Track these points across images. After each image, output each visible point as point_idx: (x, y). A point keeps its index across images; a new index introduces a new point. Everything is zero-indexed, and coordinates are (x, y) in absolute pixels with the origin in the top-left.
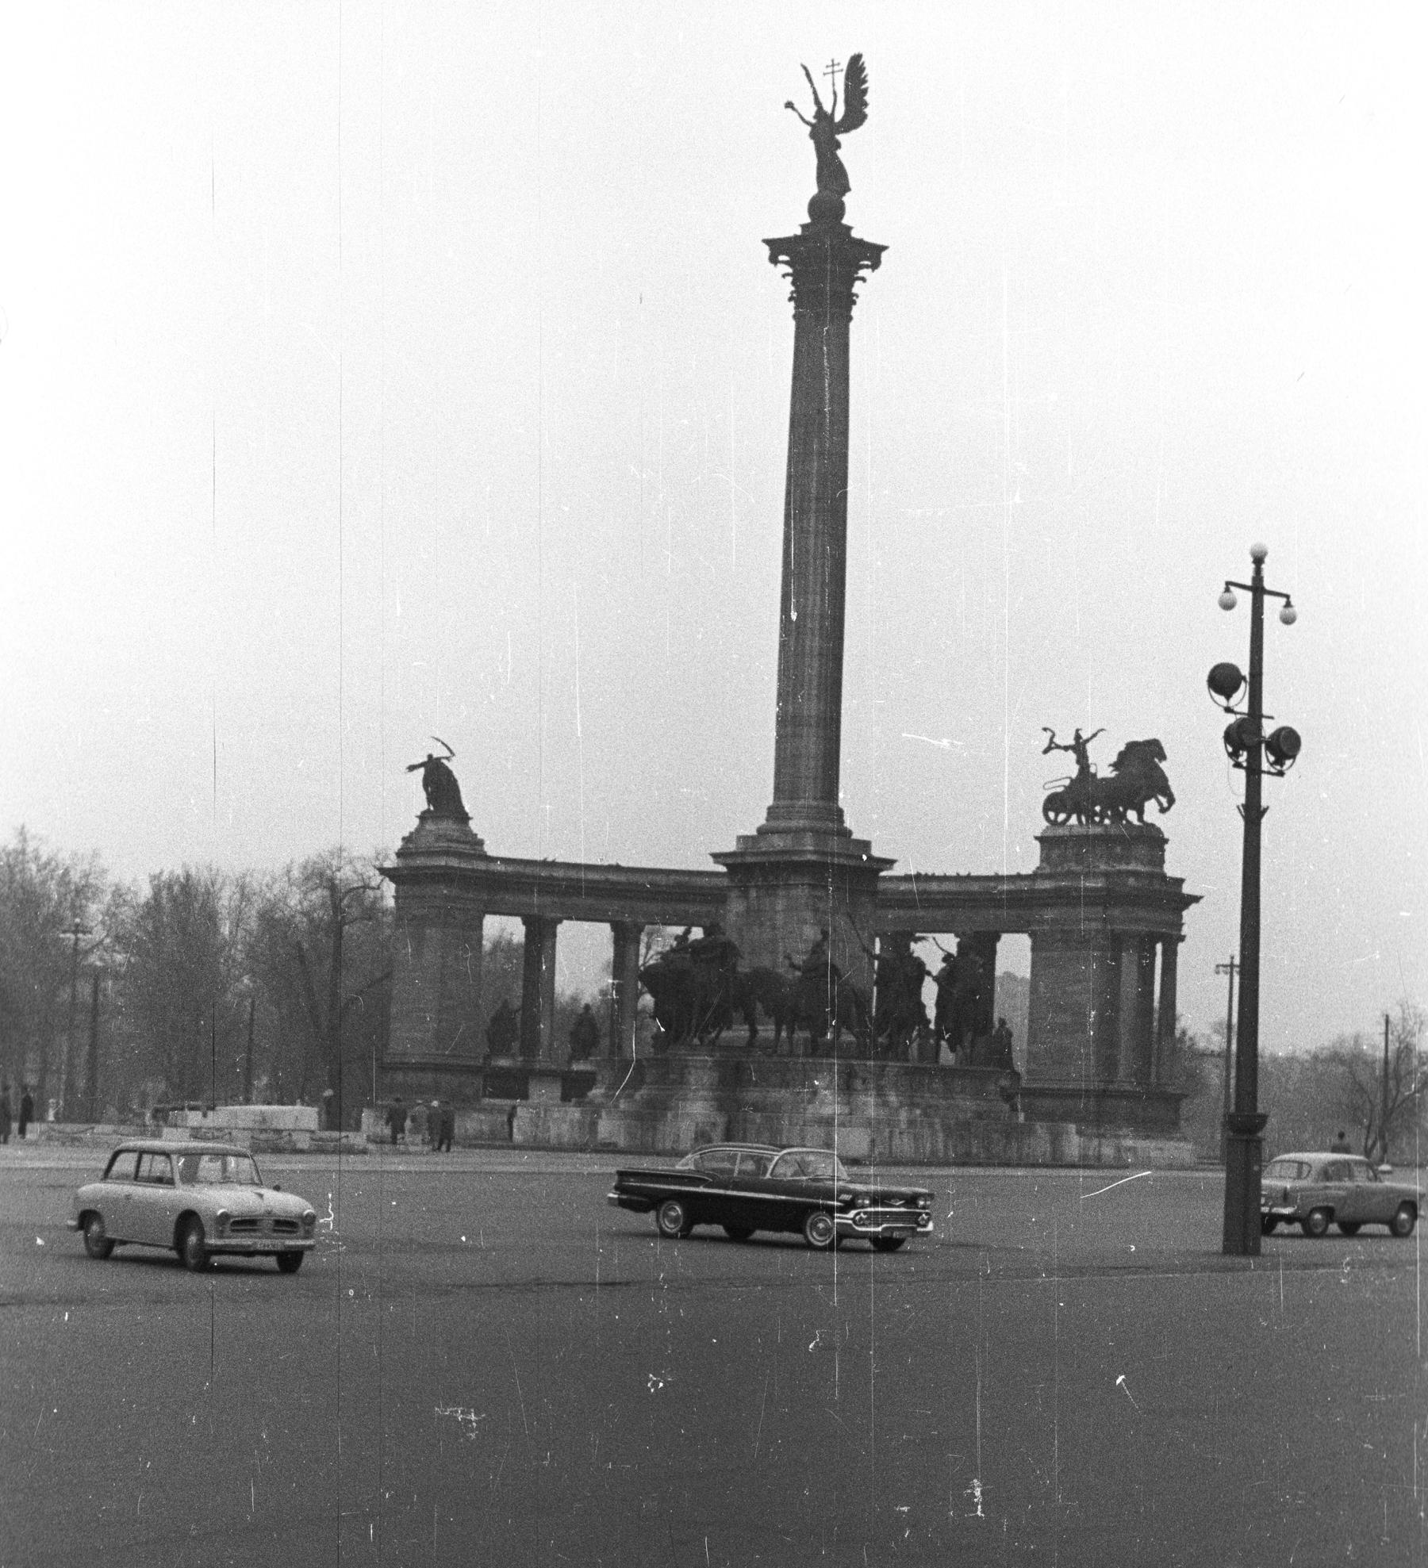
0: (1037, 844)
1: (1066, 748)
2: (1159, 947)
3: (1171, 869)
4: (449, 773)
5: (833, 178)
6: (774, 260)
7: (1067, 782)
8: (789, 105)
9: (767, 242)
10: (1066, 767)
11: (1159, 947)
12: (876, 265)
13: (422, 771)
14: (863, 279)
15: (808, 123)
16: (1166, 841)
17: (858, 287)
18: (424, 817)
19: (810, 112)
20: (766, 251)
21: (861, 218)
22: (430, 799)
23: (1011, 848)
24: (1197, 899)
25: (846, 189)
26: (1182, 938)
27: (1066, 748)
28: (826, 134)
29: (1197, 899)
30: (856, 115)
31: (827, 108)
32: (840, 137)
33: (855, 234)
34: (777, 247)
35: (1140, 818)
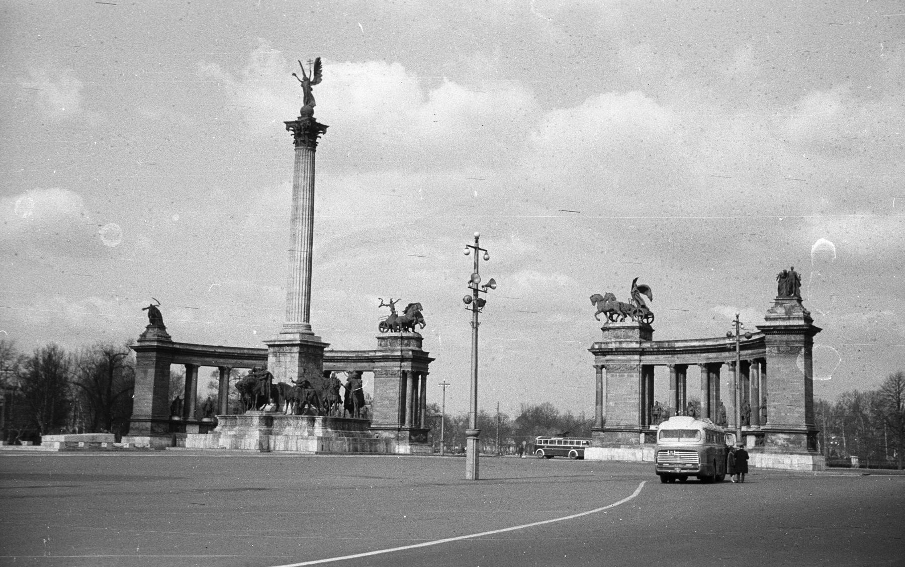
3: (424, 349)
4: (158, 311)
5: (309, 99)
8: (294, 74)
10: (387, 312)
17: (318, 140)
18: (148, 327)
19: (301, 77)
20: (285, 125)
22: (151, 321)
23: (366, 340)
24: (433, 360)
28: (307, 86)
29: (433, 360)
31: (308, 76)
32: (312, 87)
33: (317, 121)
34: (289, 124)
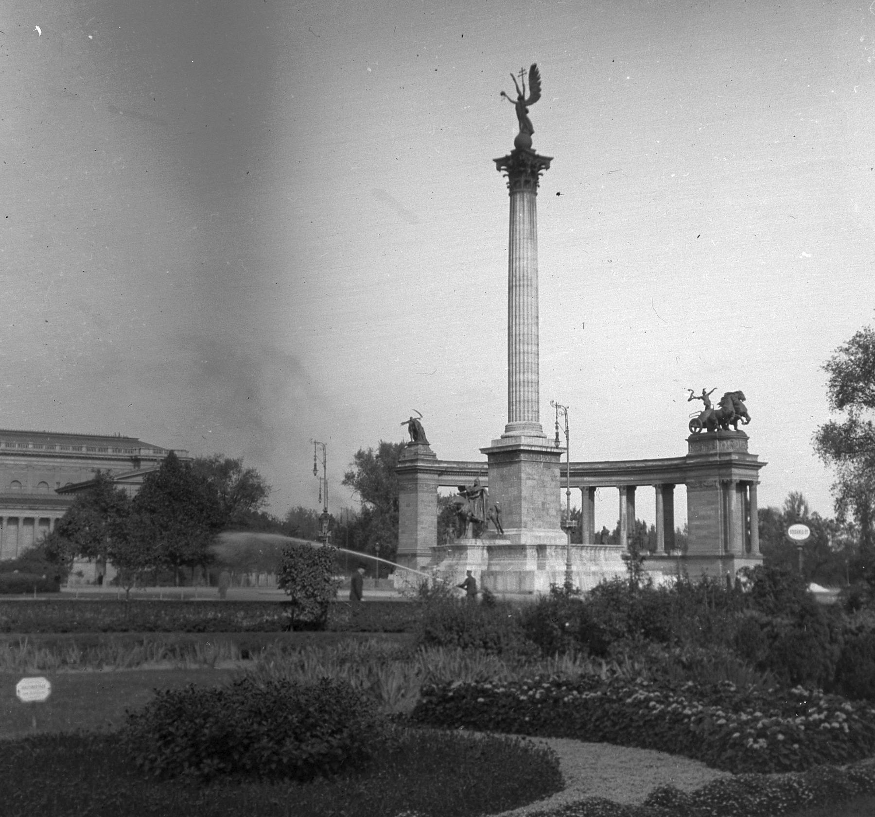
0: (687, 443)
1: (699, 398)
2: (748, 487)
5: (526, 128)
6: (499, 169)
7: (699, 414)
8: (503, 94)
9: (495, 160)
10: (700, 406)
11: (748, 487)
12: (547, 168)
13: (408, 425)
14: (542, 175)
15: (513, 102)
16: (748, 438)
20: (495, 164)
21: (540, 146)
24: (765, 464)
25: (532, 132)
26: (758, 483)
27: (699, 398)
29: (765, 464)
30: (536, 96)
32: (528, 107)
35: (736, 428)
